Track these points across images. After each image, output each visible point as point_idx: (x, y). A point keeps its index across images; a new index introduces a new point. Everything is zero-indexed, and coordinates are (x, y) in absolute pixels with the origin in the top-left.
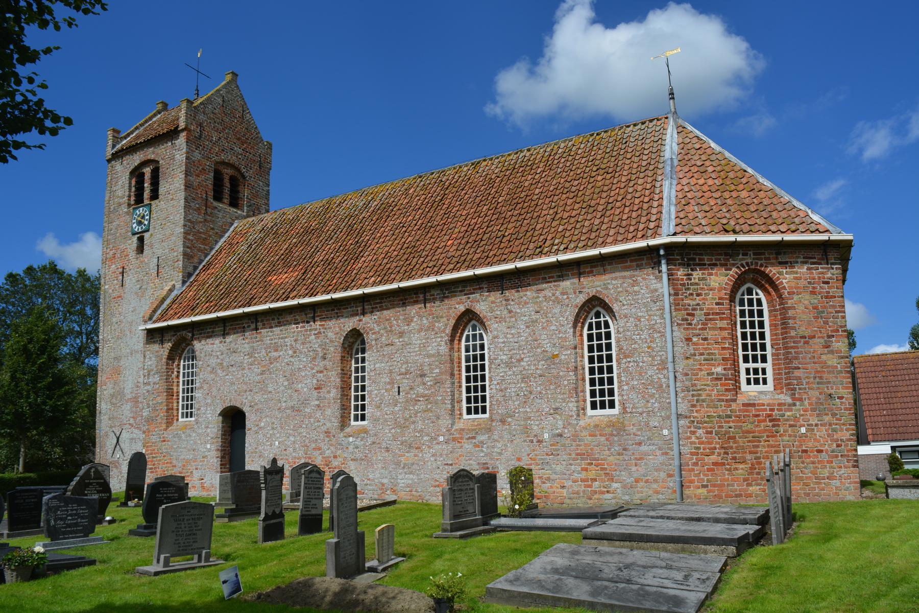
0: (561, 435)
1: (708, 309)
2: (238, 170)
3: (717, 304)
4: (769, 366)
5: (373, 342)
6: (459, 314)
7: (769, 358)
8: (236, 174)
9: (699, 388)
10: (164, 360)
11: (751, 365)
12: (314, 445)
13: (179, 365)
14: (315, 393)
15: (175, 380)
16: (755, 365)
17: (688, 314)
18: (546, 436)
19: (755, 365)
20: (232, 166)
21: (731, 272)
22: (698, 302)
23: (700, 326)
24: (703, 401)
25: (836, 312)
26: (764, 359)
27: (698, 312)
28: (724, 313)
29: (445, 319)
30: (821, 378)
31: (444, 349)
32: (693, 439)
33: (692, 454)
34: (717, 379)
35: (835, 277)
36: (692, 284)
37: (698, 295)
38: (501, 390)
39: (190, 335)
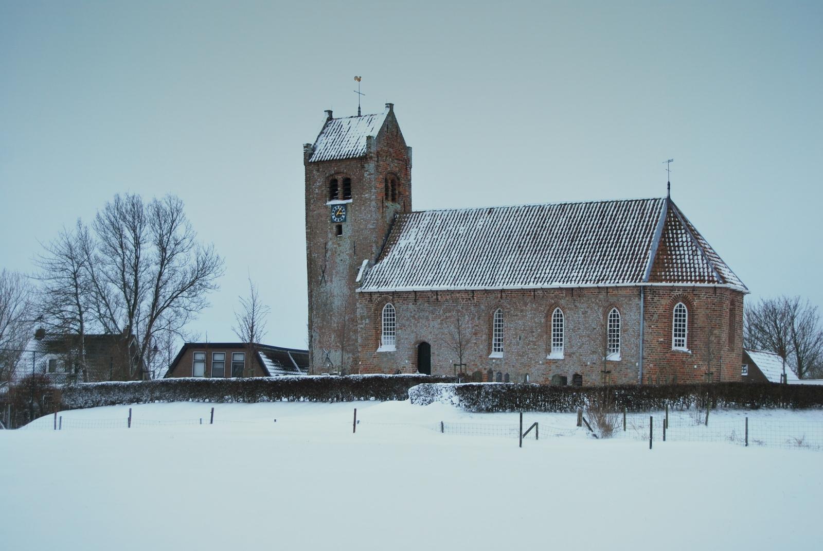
0: (594, 363)
1: (660, 314)
2: (396, 175)
3: (664, 312)
4: (685, 339)
5: (507, 313)
7: (686, 335)
11: (678, 338)
12: (473, 363)
14: (474, 337)
16: (679, 338)
18: (589, 363)
19: (679, 338)
24: (654, 352)
29: (544, 306)
31: (543, 320)
32: (648, 368)
33: (647, 373)
34: (660, 344)
38: (570, 342)
39: (391, 297)
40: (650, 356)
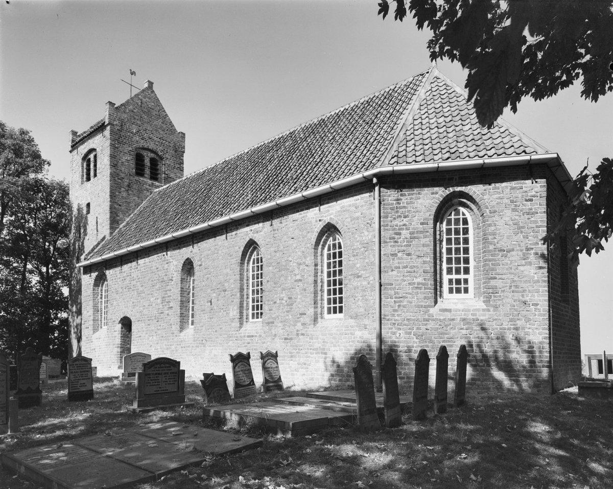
1: (413, 229)
3: (422, 224)
6: (246, 243)
8: (152, 155)
9: (400, 295)
10: (92, 287)
11: (454, 277)
13: (101, 290)
15: (100, 300)
16: (458, 277)
17: (396, 234)
19: (458, 277)
20: (152, 151)
21: (437, 196)
22: (404, 222)
23: (405, 243)
24: (404, 307)
25: (537, 227)
26: (467, 271)
27: (404, 232)
28: (428, 232)
30: (516, 287)
35: (538, 194)
36: (400, 208)
37: (405, 217)
40: (396, 313)
